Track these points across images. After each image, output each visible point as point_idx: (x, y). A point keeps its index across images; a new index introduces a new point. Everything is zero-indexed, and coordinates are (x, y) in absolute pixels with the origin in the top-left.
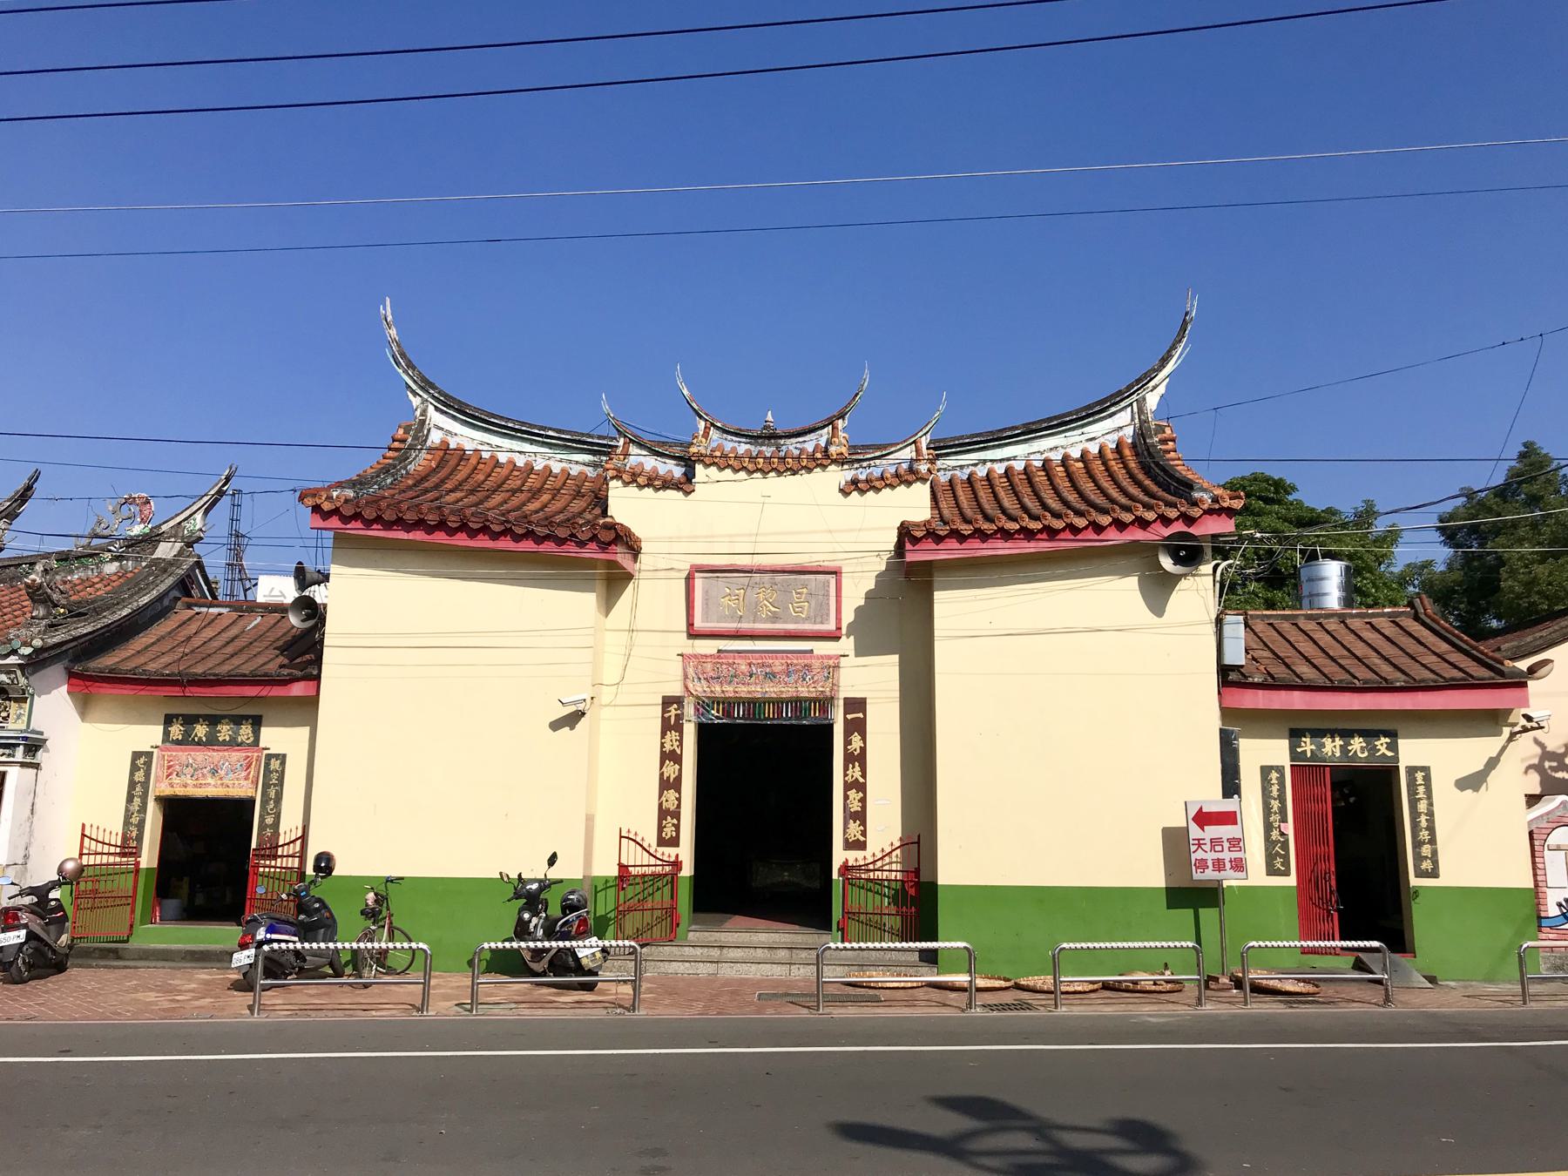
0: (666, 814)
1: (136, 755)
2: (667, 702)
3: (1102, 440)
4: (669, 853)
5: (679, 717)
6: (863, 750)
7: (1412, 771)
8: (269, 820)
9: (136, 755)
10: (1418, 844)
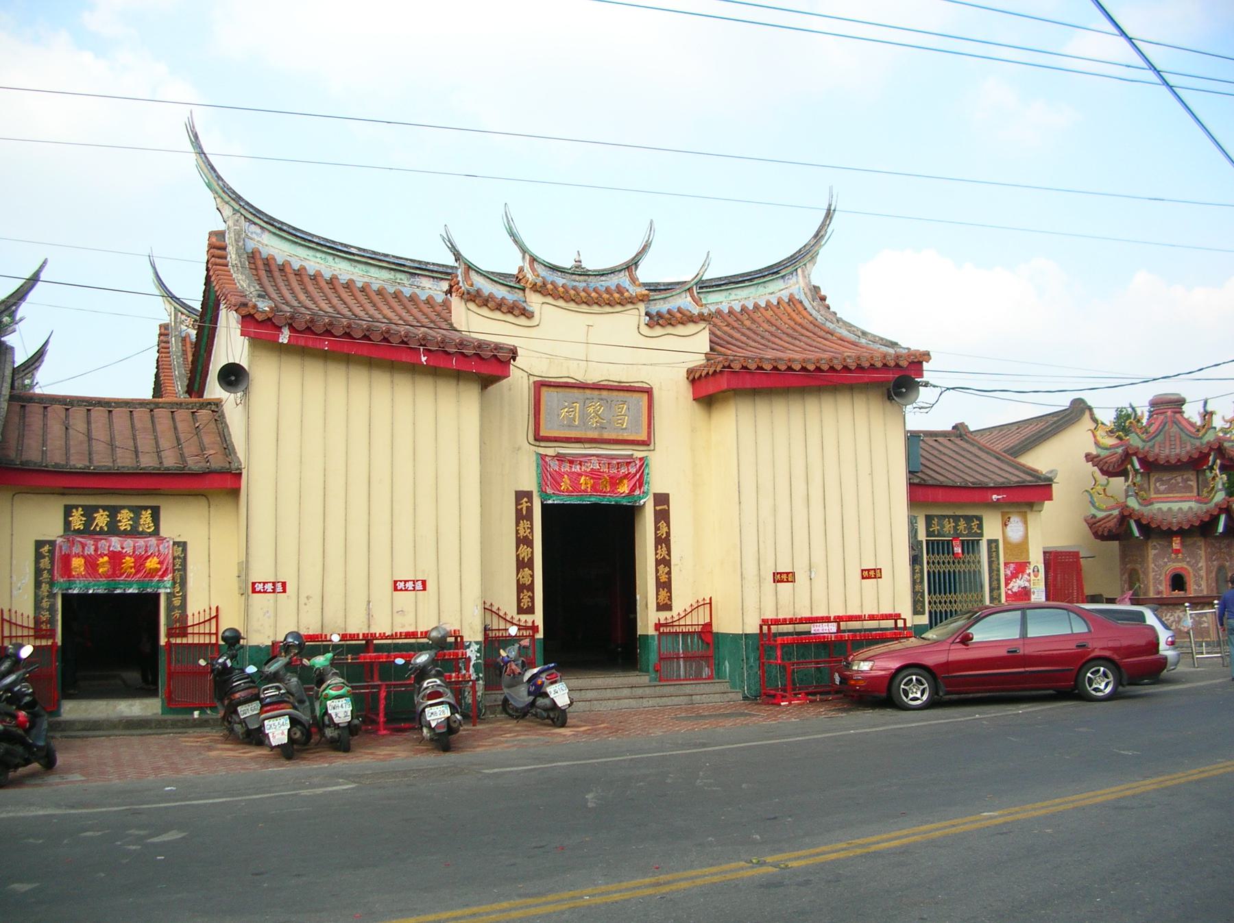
0: (524, 588)
1: (39, 544)
2: (521, 496)
3: (778, 294)
4: (526, 619)
5: (530, 510)
6: (668, 534)
7: (990, 542)
8: (177, 602)
9: (39, 544)
10: (991, 590)
